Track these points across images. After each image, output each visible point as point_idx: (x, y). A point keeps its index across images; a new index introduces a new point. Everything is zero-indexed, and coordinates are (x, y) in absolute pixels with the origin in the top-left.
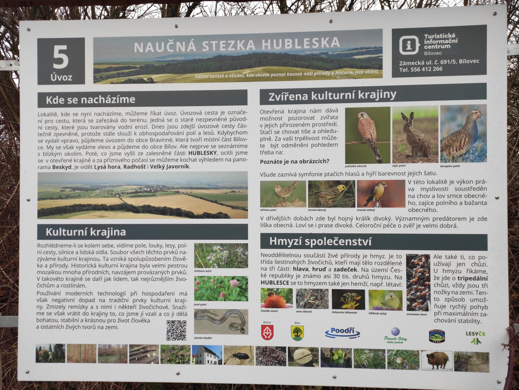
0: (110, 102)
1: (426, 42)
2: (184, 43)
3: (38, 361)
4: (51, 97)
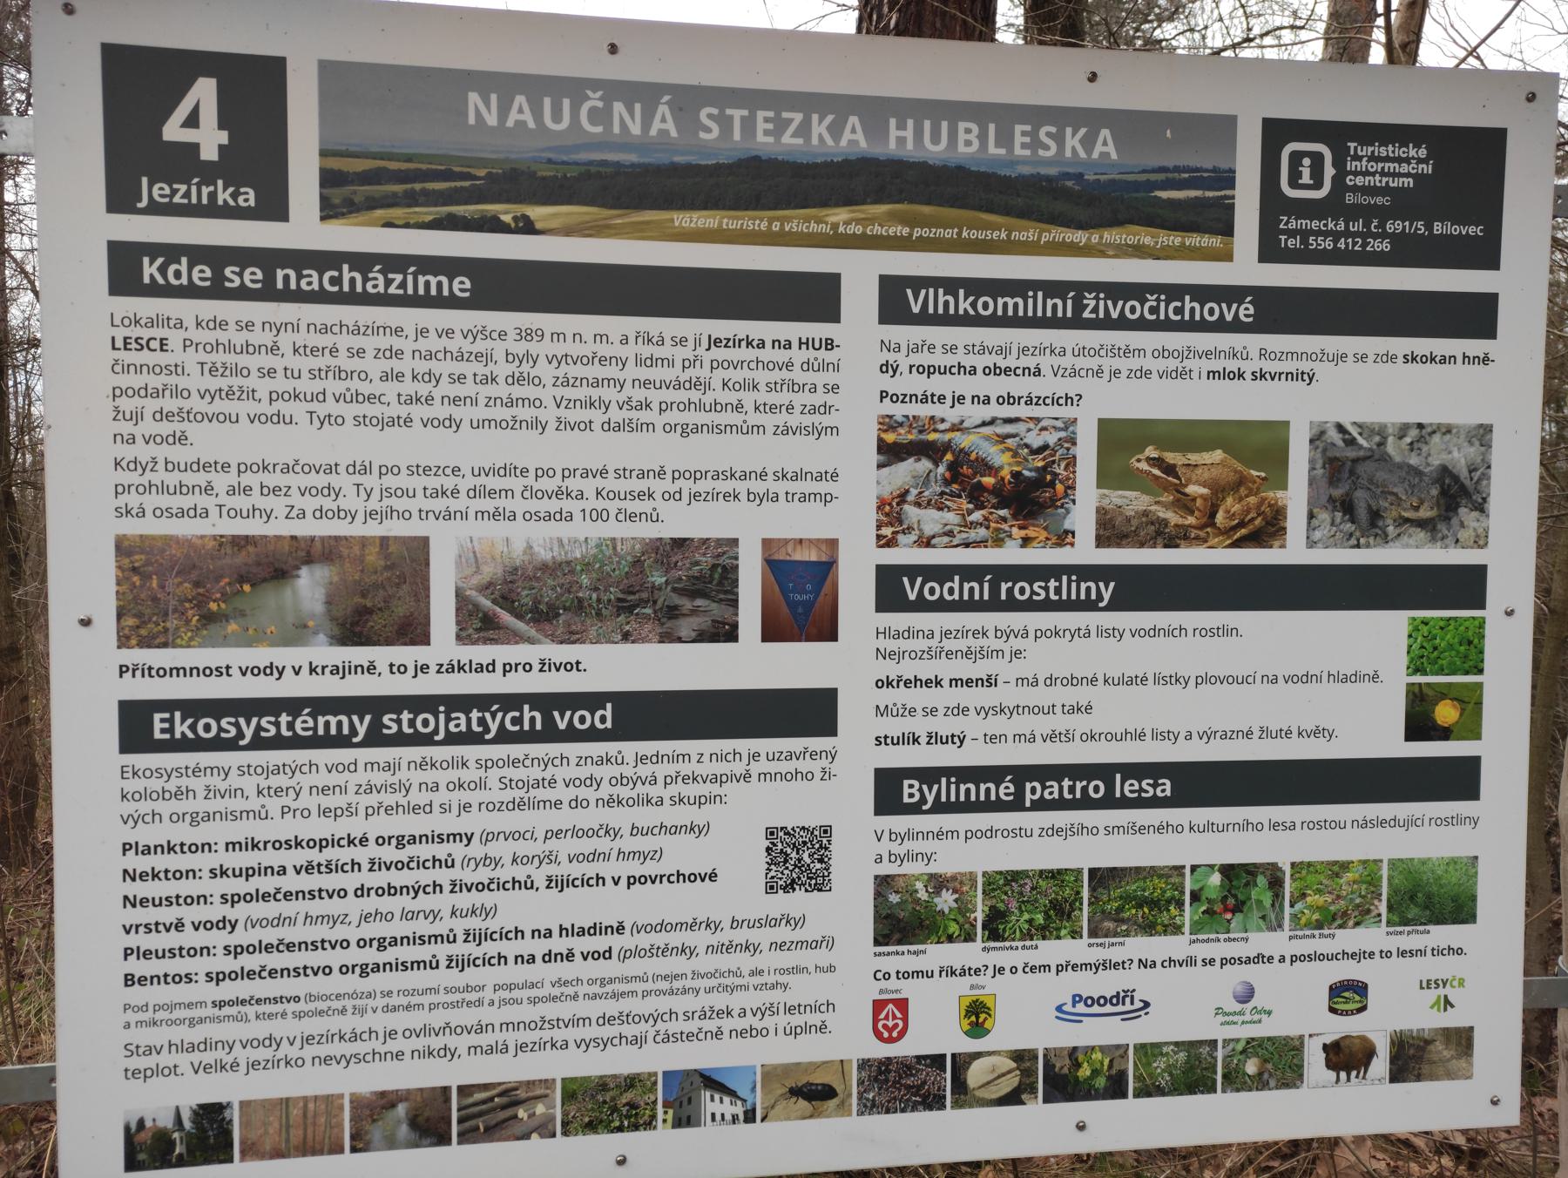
0: (381, 289)
1: (1351, 165)
2: (638, 107)
4: (160, 260)
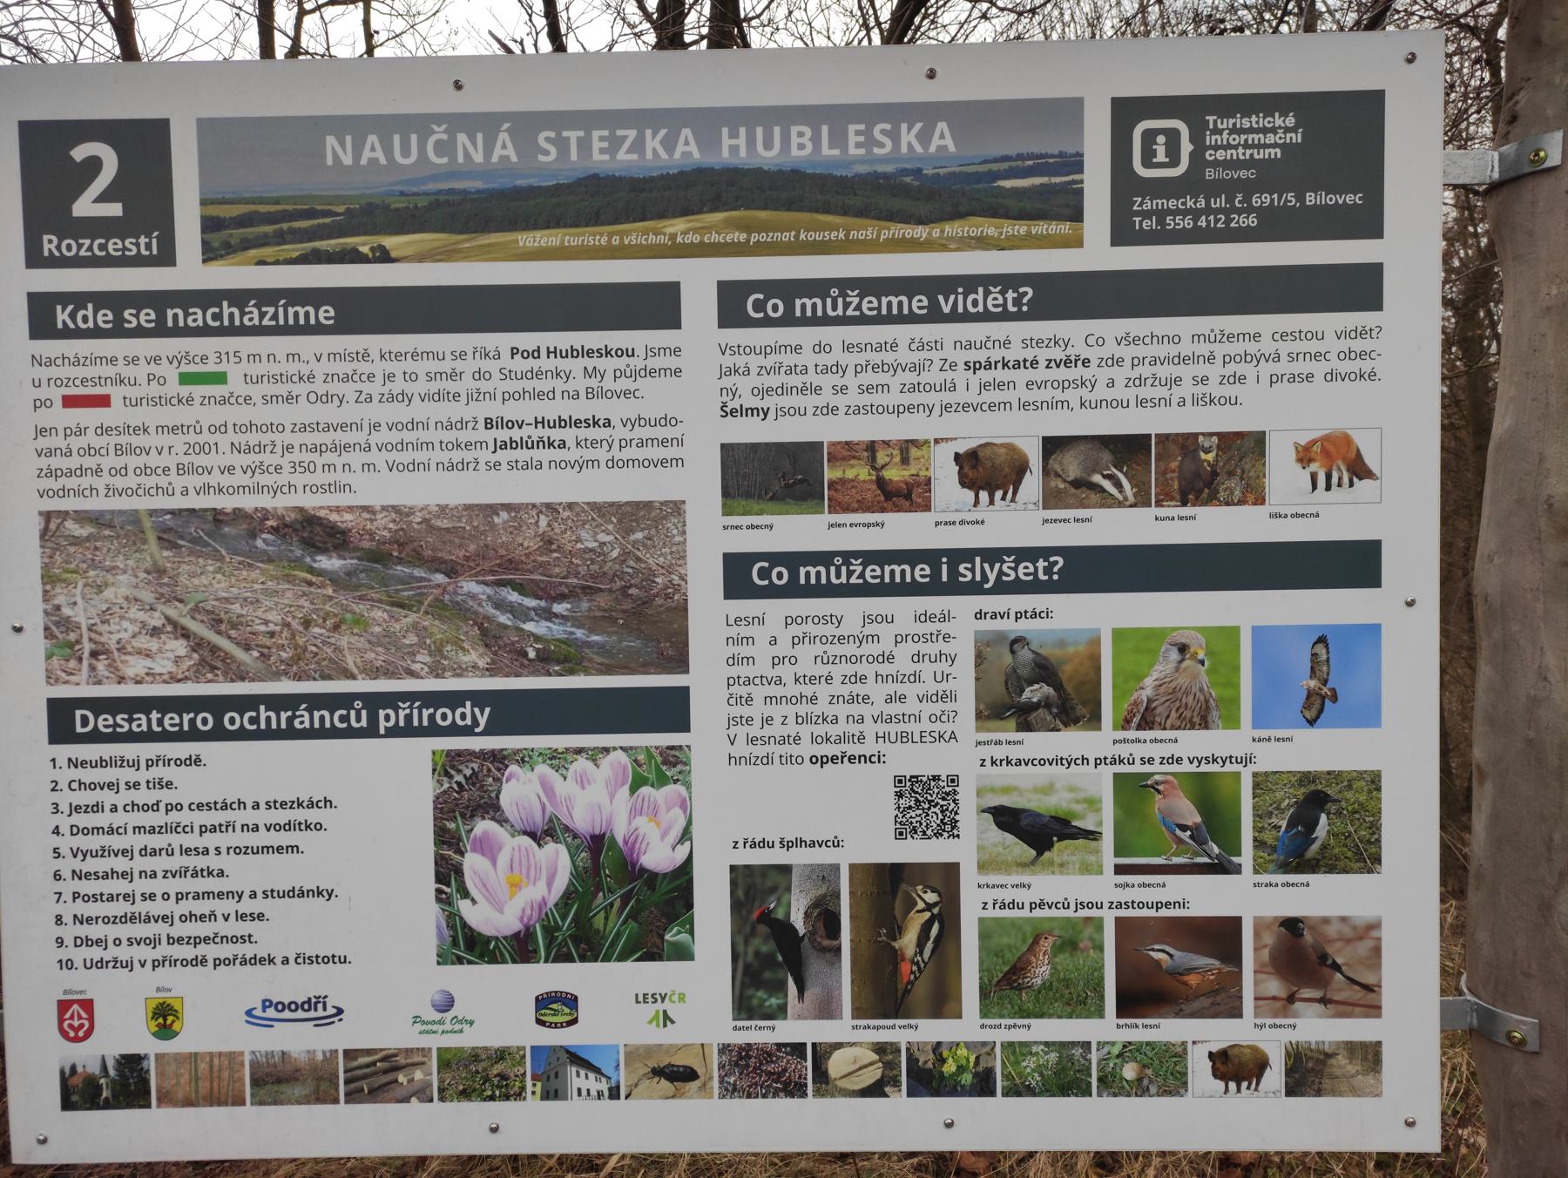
0: (256, 321)
1: (1210, 140)
2: (480, 136)
3: (67, 1105)
4: (70, 307)
